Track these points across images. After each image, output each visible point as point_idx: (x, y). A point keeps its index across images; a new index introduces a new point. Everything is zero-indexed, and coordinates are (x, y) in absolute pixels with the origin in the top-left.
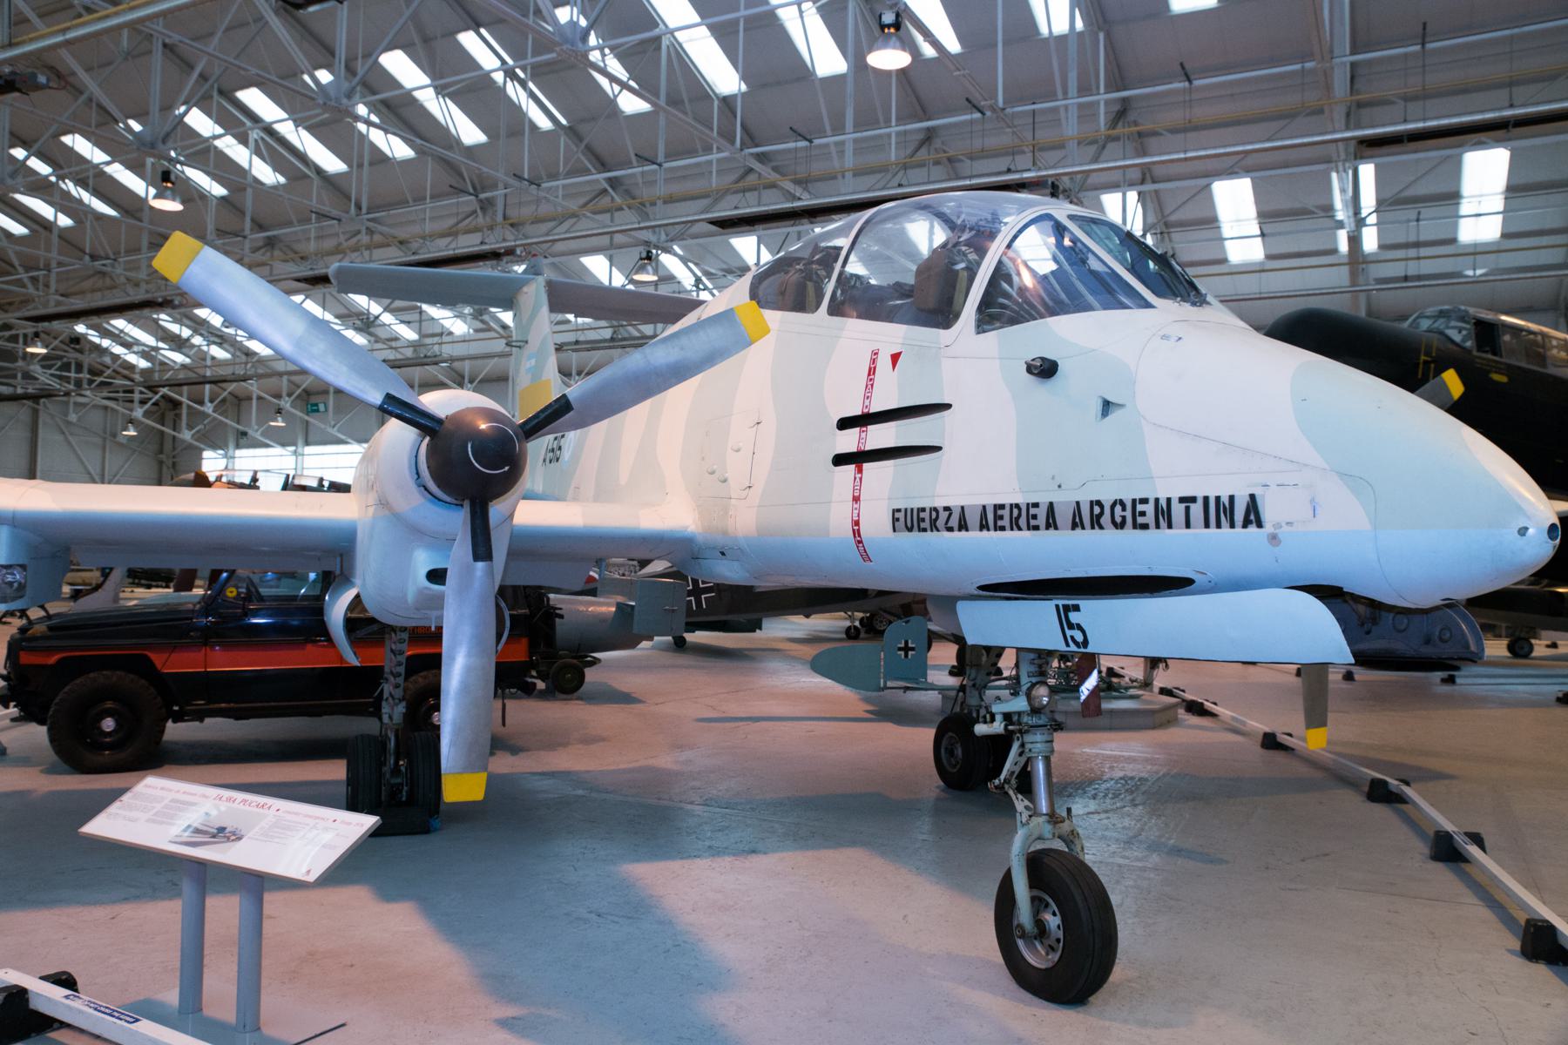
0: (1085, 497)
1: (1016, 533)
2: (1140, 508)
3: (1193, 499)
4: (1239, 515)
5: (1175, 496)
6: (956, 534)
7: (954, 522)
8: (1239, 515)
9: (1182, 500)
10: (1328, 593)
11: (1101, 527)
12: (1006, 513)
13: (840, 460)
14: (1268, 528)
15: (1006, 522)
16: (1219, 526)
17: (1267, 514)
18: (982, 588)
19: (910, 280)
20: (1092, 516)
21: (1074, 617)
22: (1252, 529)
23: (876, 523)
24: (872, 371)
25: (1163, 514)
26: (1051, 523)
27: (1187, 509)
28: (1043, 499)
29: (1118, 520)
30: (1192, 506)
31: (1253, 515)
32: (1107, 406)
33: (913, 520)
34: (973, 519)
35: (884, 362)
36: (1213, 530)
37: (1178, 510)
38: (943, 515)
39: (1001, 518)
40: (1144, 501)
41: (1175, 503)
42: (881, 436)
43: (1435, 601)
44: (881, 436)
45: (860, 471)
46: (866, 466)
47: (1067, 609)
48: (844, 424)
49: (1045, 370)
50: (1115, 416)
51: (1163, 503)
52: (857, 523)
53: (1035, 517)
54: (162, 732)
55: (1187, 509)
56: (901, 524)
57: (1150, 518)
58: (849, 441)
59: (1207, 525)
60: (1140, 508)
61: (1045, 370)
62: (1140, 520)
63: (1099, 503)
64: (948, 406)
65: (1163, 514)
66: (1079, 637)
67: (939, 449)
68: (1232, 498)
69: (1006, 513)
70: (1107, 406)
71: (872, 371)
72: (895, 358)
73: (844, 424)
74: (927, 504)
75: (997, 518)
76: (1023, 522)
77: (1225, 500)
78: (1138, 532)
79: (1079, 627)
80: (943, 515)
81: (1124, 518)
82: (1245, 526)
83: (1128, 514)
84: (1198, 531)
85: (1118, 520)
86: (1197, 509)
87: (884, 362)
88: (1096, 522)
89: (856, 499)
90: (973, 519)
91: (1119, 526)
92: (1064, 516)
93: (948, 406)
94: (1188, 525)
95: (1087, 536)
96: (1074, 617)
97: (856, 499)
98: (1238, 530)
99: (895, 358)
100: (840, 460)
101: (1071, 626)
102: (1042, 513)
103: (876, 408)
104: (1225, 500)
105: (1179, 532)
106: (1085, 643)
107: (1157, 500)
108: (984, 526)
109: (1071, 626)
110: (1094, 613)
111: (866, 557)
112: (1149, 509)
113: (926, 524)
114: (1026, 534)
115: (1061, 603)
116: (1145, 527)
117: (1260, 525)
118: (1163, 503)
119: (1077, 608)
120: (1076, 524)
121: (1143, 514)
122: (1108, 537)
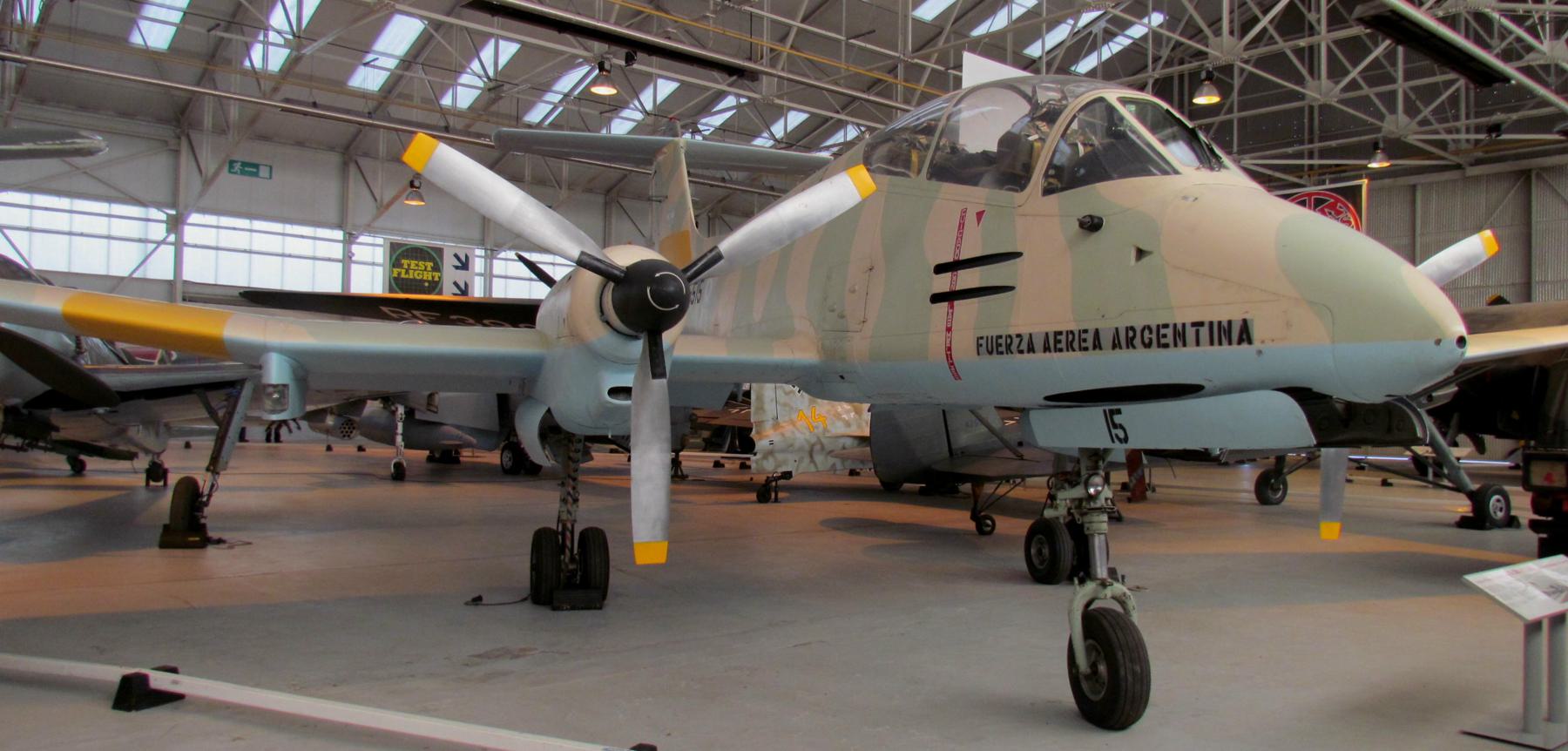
0: (1122, 324)
1: (1071, 353)
2: (1163, 331)
3: (1201, 324)
5: (1189, 320)
6: (1026, 355)
7: (1024, 346)
9: (1194, 324)
10: (1302, 395)
12: (1063, 338)
13: (936, 298)
14: (1257, 345)
15: (1063, 345)
17: (1257, 332)
18: (1047, 398)
19: (993, 148)
20: (1127, 339)
21: (1117, 419)
22: (1245, 346)
23: (964, 345)
24: (961, 226)
25: (1180, 336)
26: (1097, 345)
27: (1197, 333)
28: (1091, 327)
31: (1245, 335)
32: (1141, 253)
33: (996, 346)
34: (1039, 343)
35: (971, 217)
36: (1216, 347)
37: (1190, 332)
38: (1016, 341)
40: (1166, 326)
42: (968, 279)
43: (1377, 398)
44: (968, 279)
45: (952, 307)
46: (956, 303)
47: (1112, 412)
48: (940, 269)
49: (1092, 225)
50: (1145, 260)
51: (1180, 327)
52: (949, 349)
55: (1197, 333)
56: (983, 349)
57: (1170, 340)
58: (943, 283)
59: (1212, 343)
60: (1163, 331)
61: (1092, 225)
62: (1163, 341)
63: (1132, 328)
64: (1018, 255)
65: (1180, 336)
66: (1122, 435)
67: (1011, 288)
68: (1230, 322)
69: (1063, 338)
70: (1141, 253)
71: (961, 226)
72: (980, 215)
73: (940, 269)
74: (1004, 333)
75: (1057, 342)
76: (1076, 345)
77: (1225, 324)
79: (1121, 427)
80: (1016, 341)
83: (1154, 337)
84: (1205, 348)
86: (1204, 331)
87: (971, 217)
88: (1130, 343)
89: (949, 330)
90: (1039, 343)
91: (1148, 345)
92: (1106, 340)
93: (1018, 255)
94: (1198, 344)
95: (1124, 355)
96: (1117, 419)
97: (949, 330)
98: (1235, 347)
99: (980, 215)
100: (936, 298)
101: (1115, 426)
102: (1090, 337)
103: (965, 255)
104: (1225, 324)
105: (1191, 349)
106: (1126, 440)
108: (1046, 349)
109: (1115, 426)
110: (1130, 413)
111: (957, 376)
112: (1169, 332)
113: (1003, 349)
114: (1078, 354)
116: (1166, 346)
117: (1250, 342)
118: (1180, 327)
119: (1119, 412)
120: (1116, 345)
121: (1165, 336)
122: (1139, 355)
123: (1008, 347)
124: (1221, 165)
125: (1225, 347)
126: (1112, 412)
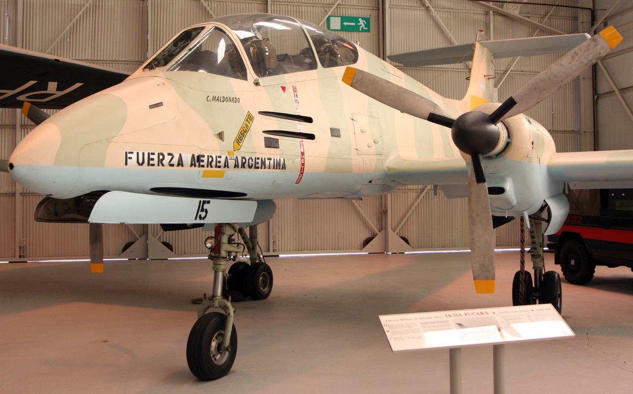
2: (257, 161)
4: (281, 167)
6: (175, 168)
7: (175, 161)
8: (281, 167)
11: (244, 168)
16: (277, 169)
21: (206, 206)
22: (283, 170)
29: (250, 165)
30: (271, 161)
31: (284, 167)
36: (275, 170)
38: (167, 158)
39: (203, 161)
40: (258, 159)
41: (266, 159)
53: (219, 162)
54: (594, 272)
69: (205, 159)
76: (214, 164)
78: (256, 170)
81: (252, 164)
82: (282, 169)
83: (254, 163)
85: (250, 165)
88: (243, 166)
91: (250, 167)
96: (206, 206)
107: (262, 158)
115: (202, 200)
118: (263, 159)
119: (209, 202)
122: (246, 171)
123: (160, 162)
124: (244, 77)
125: (278, 170)
126: (204, 202)
